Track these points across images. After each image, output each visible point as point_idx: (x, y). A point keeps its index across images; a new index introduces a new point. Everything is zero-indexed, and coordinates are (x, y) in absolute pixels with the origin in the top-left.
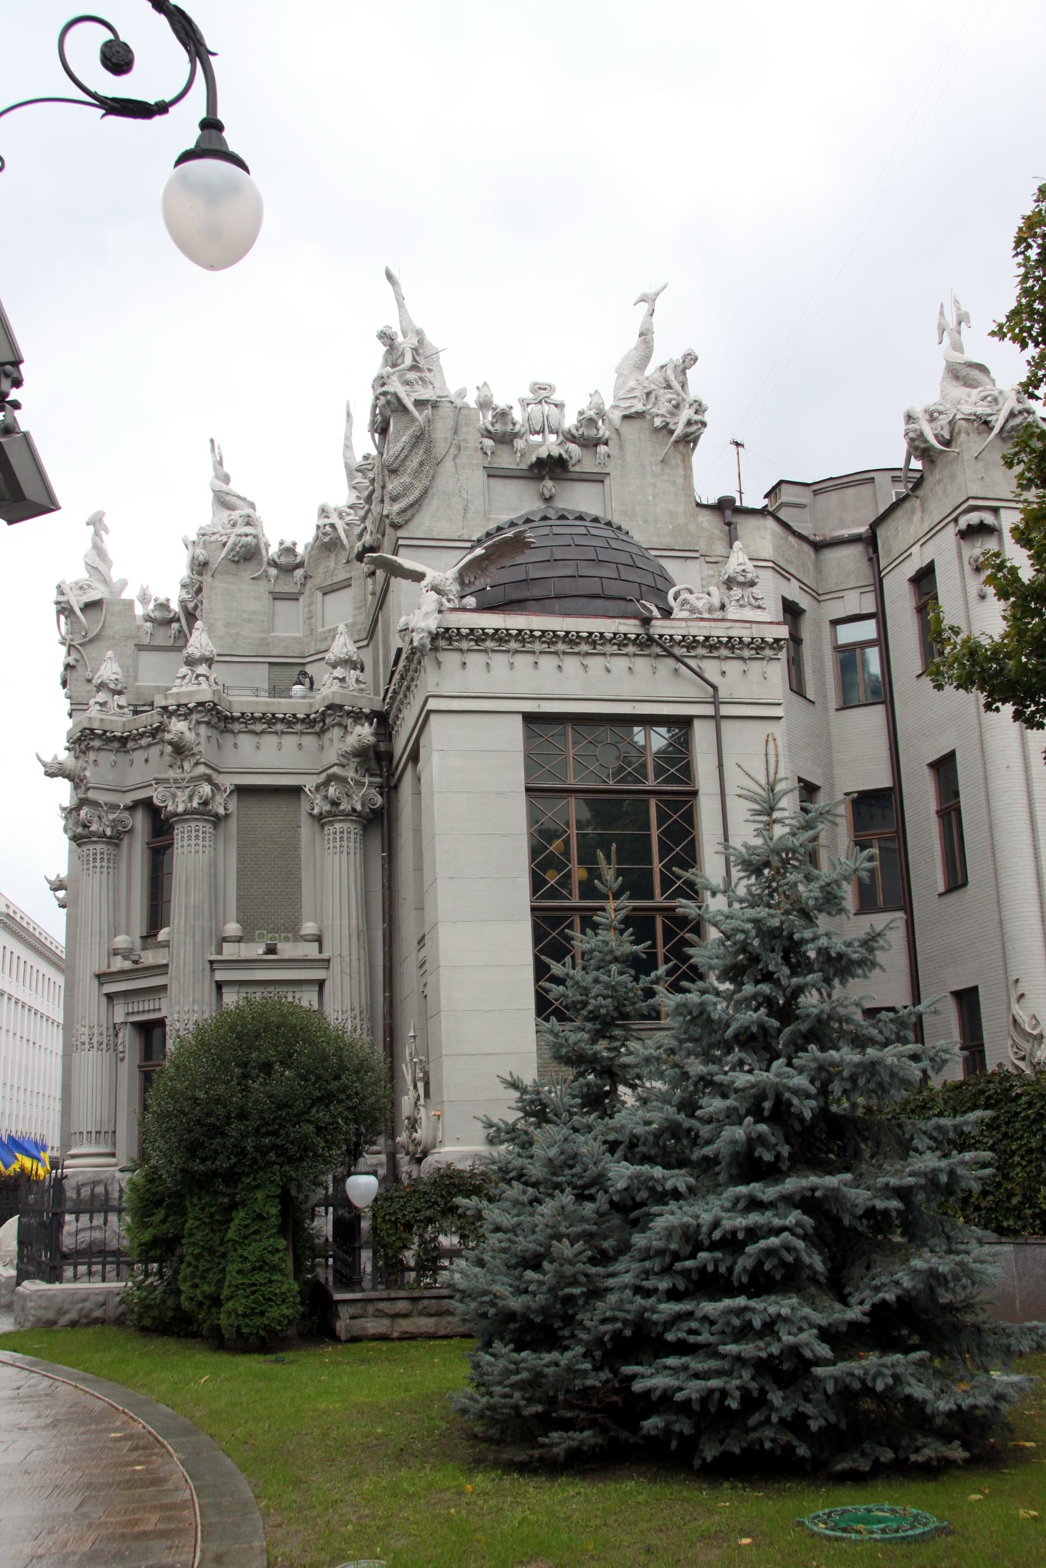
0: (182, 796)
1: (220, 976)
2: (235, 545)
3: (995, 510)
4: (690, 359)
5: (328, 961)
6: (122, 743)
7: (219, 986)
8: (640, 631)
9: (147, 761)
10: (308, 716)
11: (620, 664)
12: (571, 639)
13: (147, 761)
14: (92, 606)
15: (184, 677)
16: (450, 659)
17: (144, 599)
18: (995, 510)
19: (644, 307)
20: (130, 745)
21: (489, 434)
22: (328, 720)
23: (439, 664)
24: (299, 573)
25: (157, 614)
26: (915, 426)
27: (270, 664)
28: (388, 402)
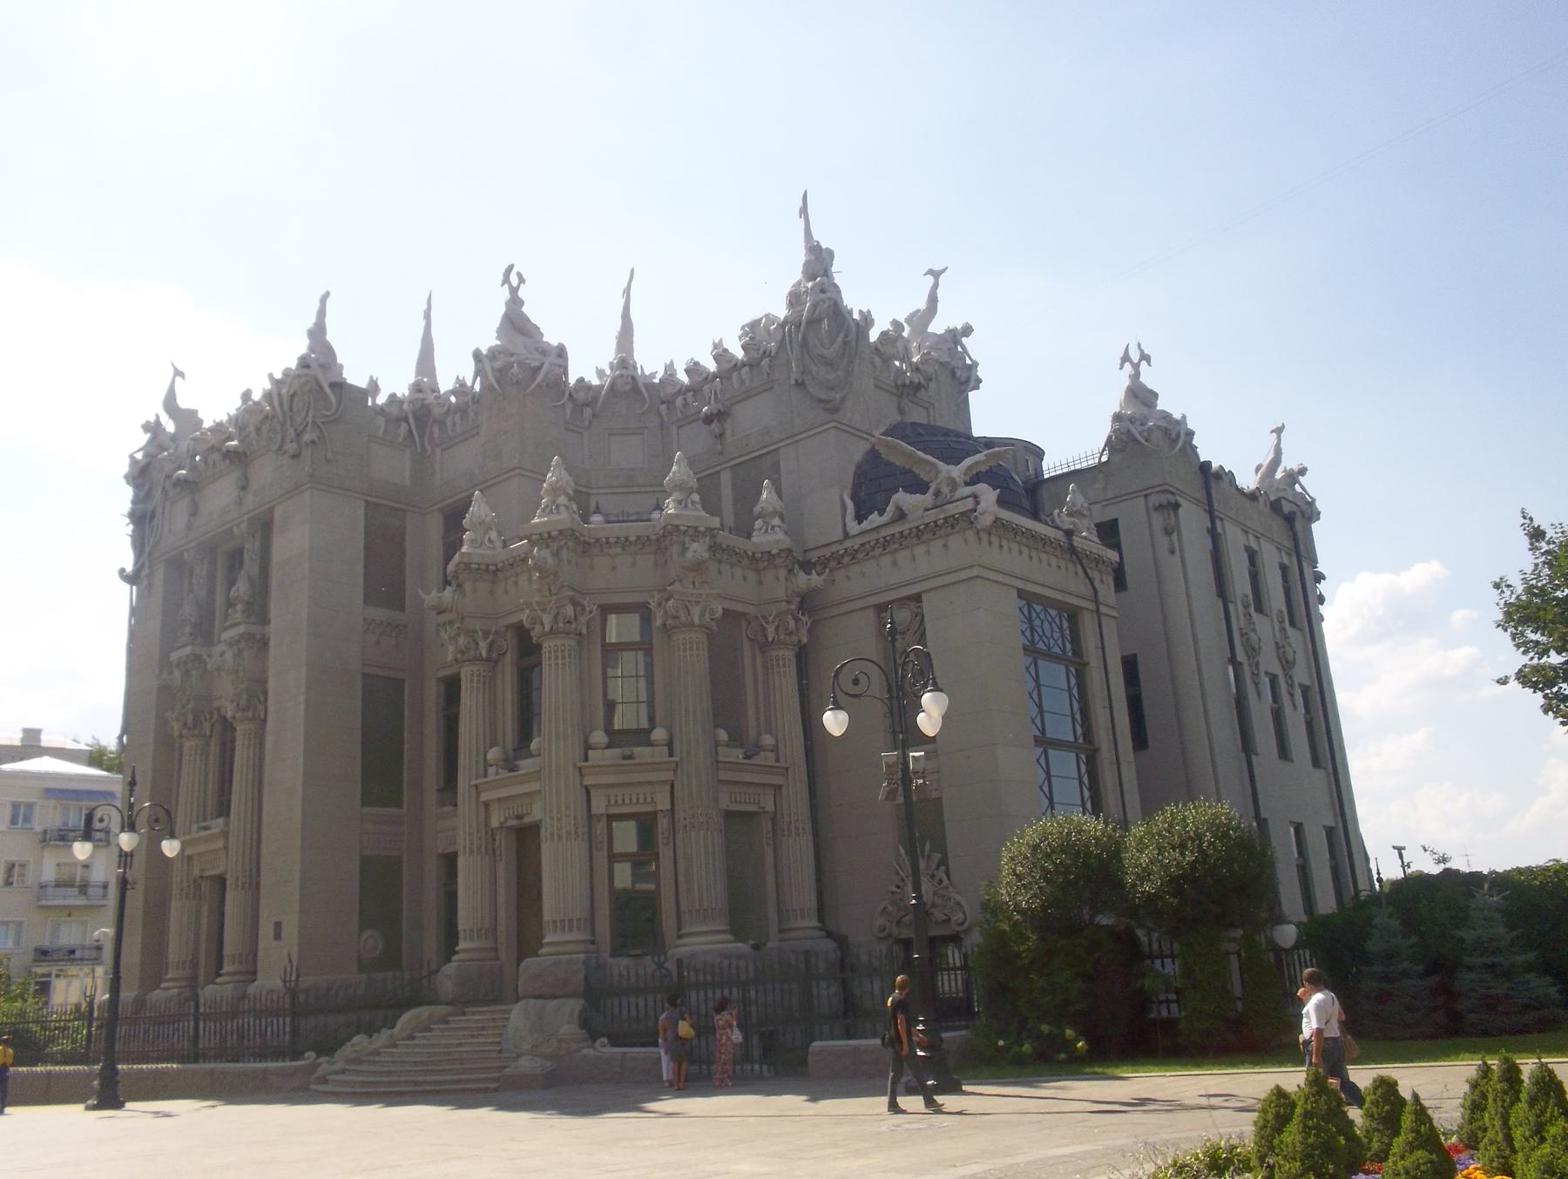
0: (696, 611)
1: (723, 775)
2: (548, 373)
4: (967, 331)
6: (586, 547)
7: (720, 781)
9: (614, 568)
11: (1054, 561)
13: (614, 568)
14: (332, 385)
15: (680, 502)
16: (984, 536)
17: (374, 387)
21: (876, 349)
22: (778, 561)
24: (588, 412)
25: (395, 411)
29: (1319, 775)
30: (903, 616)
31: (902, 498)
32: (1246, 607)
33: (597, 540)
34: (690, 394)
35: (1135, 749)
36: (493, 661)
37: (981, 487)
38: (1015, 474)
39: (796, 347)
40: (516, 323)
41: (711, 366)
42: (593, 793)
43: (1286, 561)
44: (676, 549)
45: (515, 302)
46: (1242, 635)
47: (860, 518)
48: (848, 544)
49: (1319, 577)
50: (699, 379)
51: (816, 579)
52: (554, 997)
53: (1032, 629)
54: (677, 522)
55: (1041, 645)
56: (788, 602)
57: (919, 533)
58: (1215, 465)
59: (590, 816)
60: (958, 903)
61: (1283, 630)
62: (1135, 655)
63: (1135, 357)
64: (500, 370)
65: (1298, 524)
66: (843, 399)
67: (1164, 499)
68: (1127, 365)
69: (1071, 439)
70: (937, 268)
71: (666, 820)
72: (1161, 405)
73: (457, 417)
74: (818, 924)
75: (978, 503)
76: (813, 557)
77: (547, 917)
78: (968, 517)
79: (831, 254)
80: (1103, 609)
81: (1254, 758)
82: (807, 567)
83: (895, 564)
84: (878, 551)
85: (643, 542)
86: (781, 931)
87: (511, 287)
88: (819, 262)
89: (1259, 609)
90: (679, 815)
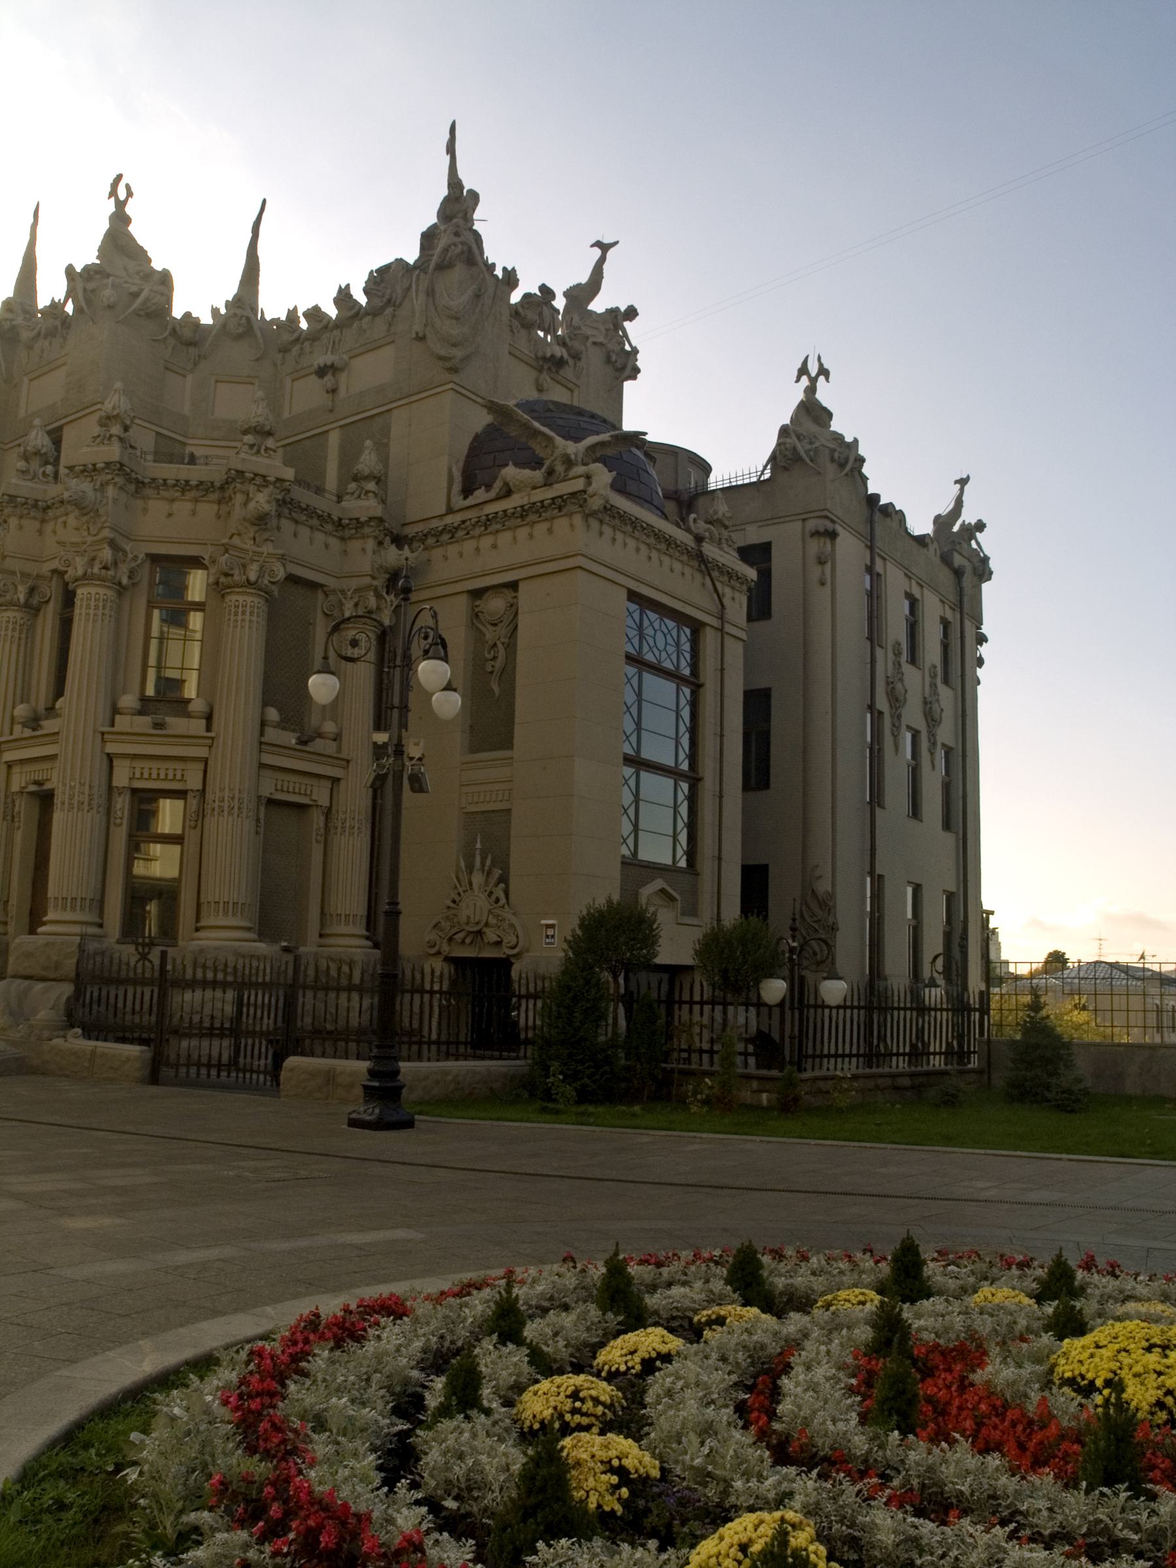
1: (268, 759)
2: (147, 299)
3: (833, 522)
4: (631, 313)
5: (348, 761)
7: (262, 766)
8: (693, 545)
9: (170, 515)
10: (340, 519)
11: (678, 566)
12: (658, 536)
13: (170, 515)
15: (252, 446)
16: (594, 524)
18: (833, 522)
19: (597, 252)
20: (148, 492)
22: (367, 530)
23: (588, 526)
26: (788, 440)
27: (158, 433)
28: (462, 252)
29: (949, 840)
30: (495, 605)
31: (511, 472)
32: (897, 654)
33: (154, 480)
34: (307, 344)
35: (746, 787)
36: (33, 609)
37: (597, 467)
38: (667, 480)
39: (422, 297)
40: (119, 240)
41: (332, 312)
42: (116, 762)
43: (949, 615)
44: (239, 498)
45: (120, 219)
46: (888, 683)
47: (467, 492)
48: (449, 520)
49: (982, 639)
50: (320, 326)
51: (406, 551)
52: (43, 979)
53: (642, 636)
54: (240, 468)
55: (649, 657)
56: (374, 578)
57: (523, 513)
58: (883, 501)
59: (110, 788)
60: (512, 925)
61: (933, 685)
62: (770, 689)
63: (813, 369)
64: (93, 291)
65: (967, 580)
66: (467, 358)
67: (823, 525)
68: (804, 379)
69: (738, 453)
70: (606, 241)
71: (195, 802)
72: (836, 426)
73: (47, 343)
74: (365, 933)
75: (590, 484)
76: (410, 531)
77: (49, 895)
78: (578, 497)
79: (474, 197)
80: (728, 628)
81: (878, 811)
82: (399, 541)
83: (495, 546)
84: (477, 531)
85: (205, 488)
86: (321, 936)
87: (118, 201)
88: (459, 205)
89: (913, 660)
90: (209, 797)
